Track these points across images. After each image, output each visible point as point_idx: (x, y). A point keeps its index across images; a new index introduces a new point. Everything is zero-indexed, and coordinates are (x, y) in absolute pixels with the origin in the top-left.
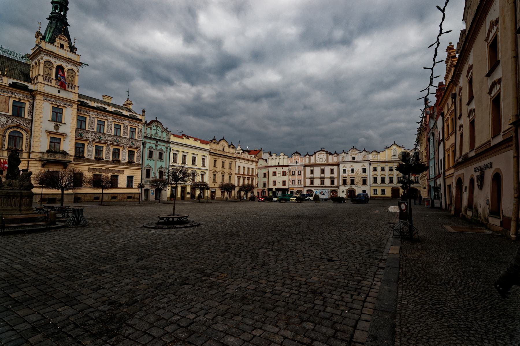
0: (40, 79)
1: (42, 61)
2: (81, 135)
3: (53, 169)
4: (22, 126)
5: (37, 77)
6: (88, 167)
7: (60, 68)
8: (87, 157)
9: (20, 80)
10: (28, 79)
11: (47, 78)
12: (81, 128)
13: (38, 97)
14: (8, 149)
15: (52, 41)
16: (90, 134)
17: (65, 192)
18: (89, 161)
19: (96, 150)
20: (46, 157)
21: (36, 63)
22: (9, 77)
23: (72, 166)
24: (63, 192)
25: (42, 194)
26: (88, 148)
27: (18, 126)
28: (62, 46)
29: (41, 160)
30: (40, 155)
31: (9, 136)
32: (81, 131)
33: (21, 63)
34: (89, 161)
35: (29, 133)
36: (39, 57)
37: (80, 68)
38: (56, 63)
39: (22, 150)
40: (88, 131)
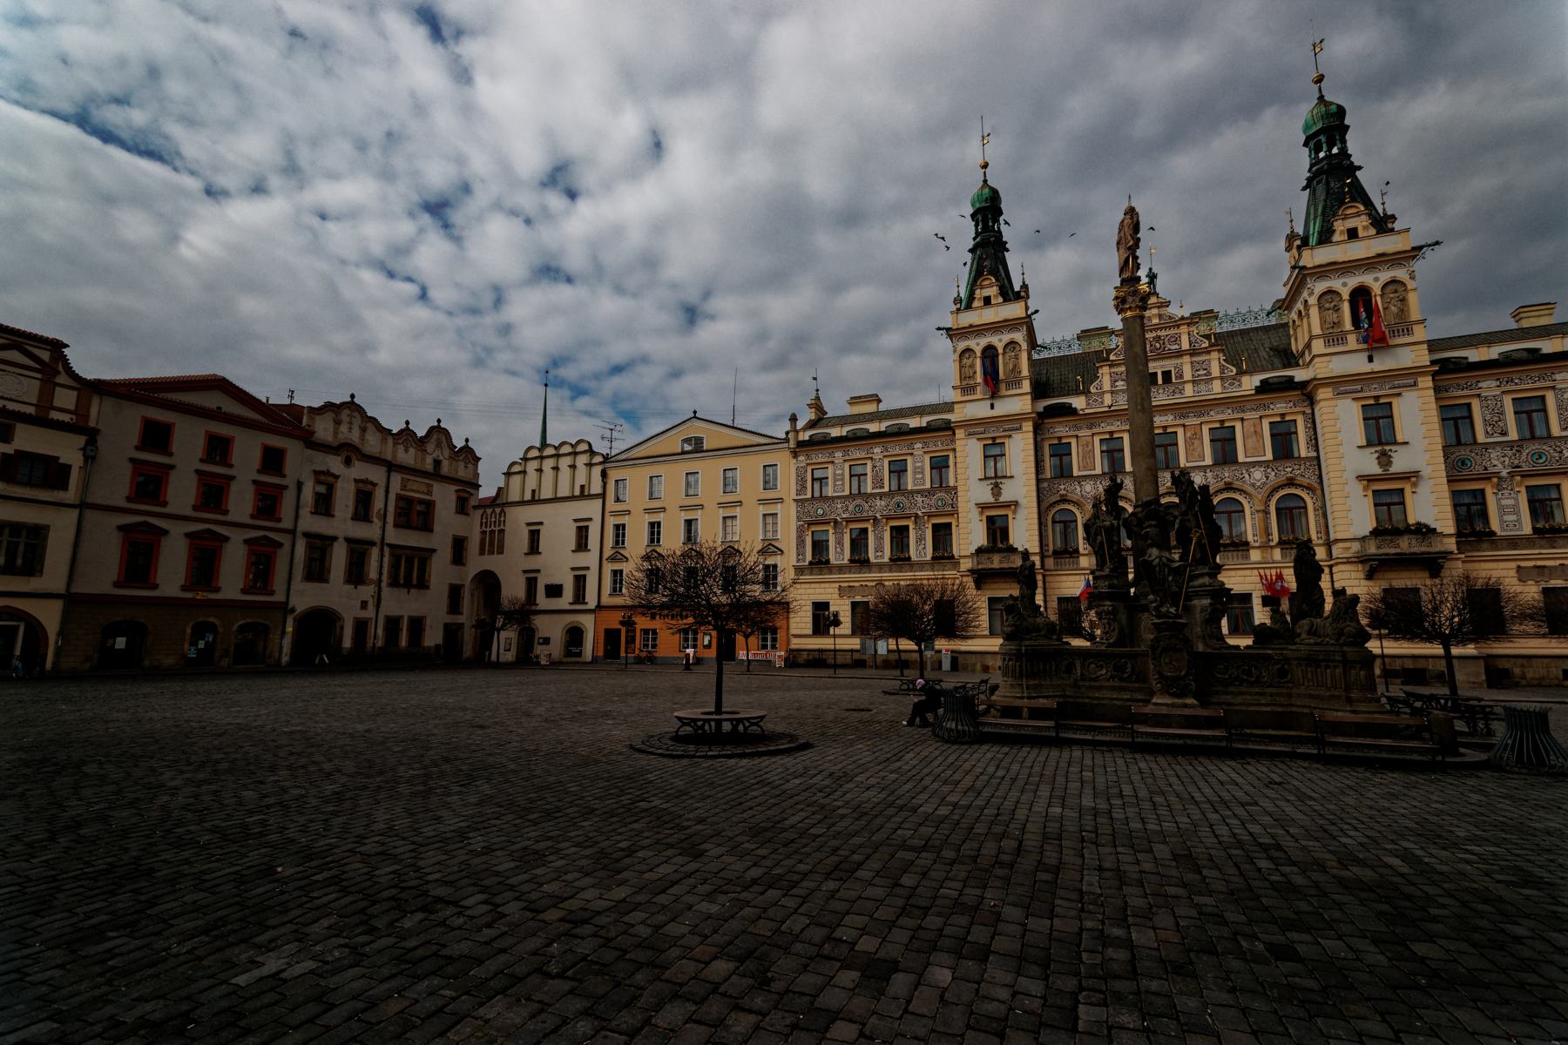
0: (1318, 346)
1: (1313, 301)
2: (1463, 463)
3: (1403, 580)
4: (1300, 480)
5: (1308, 346)
6: (1513, 565)
7: (1361, 296)
8: (1502, 529)
9: (1274, 369)
10: (1289, 358)
11: (1333, 336)
12: (1459, 443)
13: (1323, 394)
14: (1281, 543)
15: (1325, 237)
16: (1494, 454)
17: (1455, 651)
18: (1513, 542)
19: (1531, 502)
20: (1372, 549)
21: (1300, 312)
22: (1250, 372)
23: (1456, 569)
24: (1447, 650)
25: (1383, 656)
26: (1498, 500)
27: (1291, 482)
28: (1353, 234)
29: (1362, 559)
30: (1356, 546)
31: (1277, 509)
32: (1463, 452)
33: (1266, 329)
34: (1513, 542)
35: (1319, 492)
36: (1305, 294)
37: (1418, 265)
38: (1344, 286)
39: (1310, 540)
40: (1486, 446)
